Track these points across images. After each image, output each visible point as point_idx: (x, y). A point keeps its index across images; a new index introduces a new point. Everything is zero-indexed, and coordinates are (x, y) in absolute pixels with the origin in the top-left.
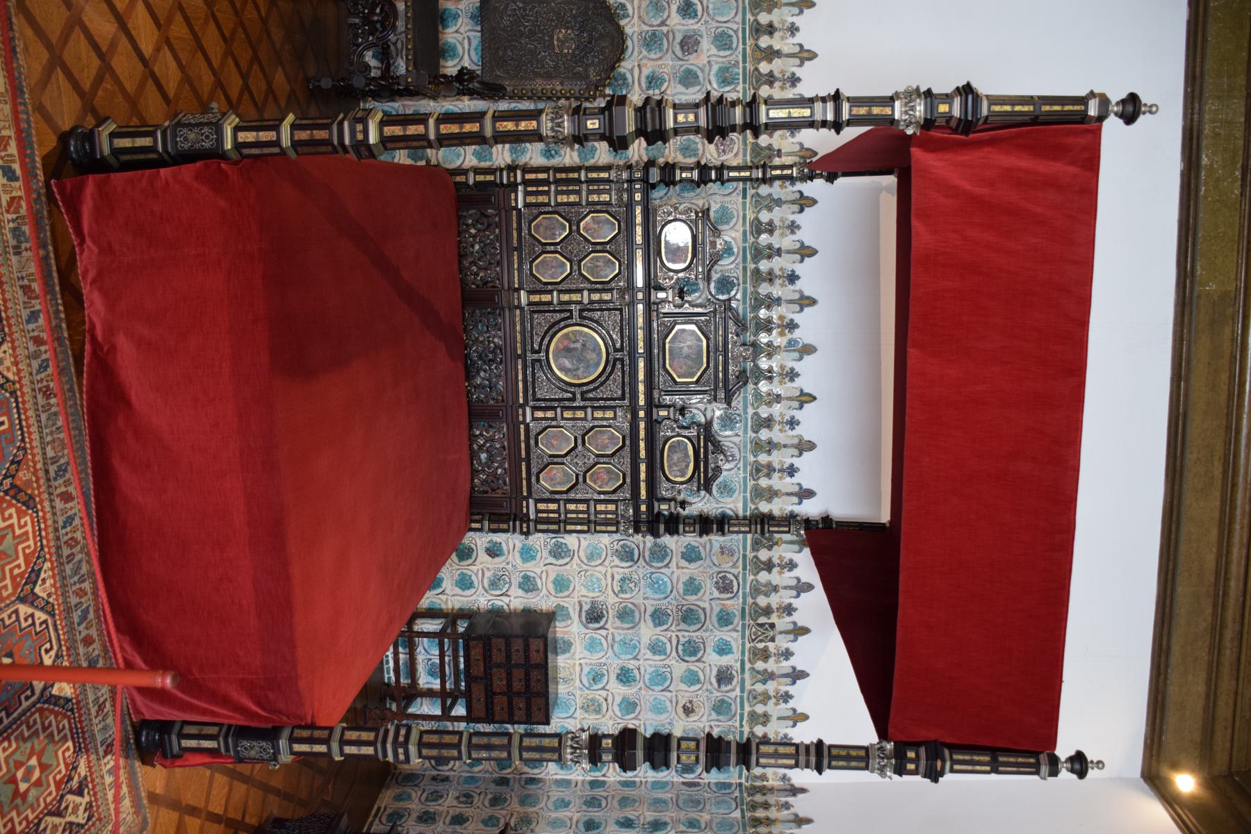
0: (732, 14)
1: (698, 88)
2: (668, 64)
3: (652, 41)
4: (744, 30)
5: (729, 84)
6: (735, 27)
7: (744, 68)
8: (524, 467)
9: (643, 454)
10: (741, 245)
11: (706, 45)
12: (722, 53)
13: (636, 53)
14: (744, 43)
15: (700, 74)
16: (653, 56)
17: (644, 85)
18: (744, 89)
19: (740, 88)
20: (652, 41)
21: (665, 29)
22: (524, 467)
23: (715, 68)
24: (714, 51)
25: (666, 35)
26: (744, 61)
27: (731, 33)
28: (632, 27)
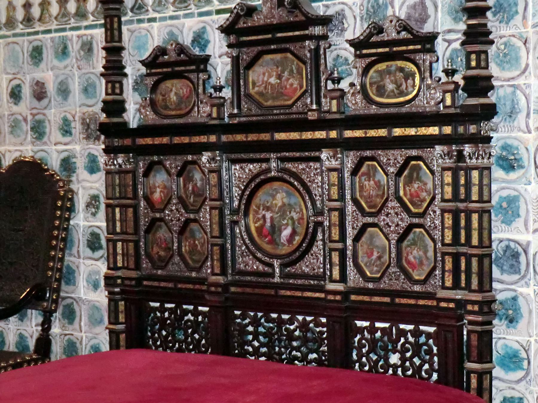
0: (17, 48)
1: (70, 79)
2: (53, 115)
3: (38, 130)
4: (29, 34)
5: (65, 47)
6: (26, 44)
7: (56, 31)
8: (404, 301)
9: (382, 132)
10: (197, 19)
11: (39, 75)
12: (44, 56)
13: (45, 147)
14: (37, 33)
15: (59, 80)
16: (47, 130)
17: (67, 139)
18: (72, 29)
19: (69, 33)
20: (38, 130)
21: (29, 118)
22: (404, 301)
23: (56, 62)
24: (43, 65)
25: (34, 115)
26: (49, 31)
27: (31, 49)
28: (28, 150)
